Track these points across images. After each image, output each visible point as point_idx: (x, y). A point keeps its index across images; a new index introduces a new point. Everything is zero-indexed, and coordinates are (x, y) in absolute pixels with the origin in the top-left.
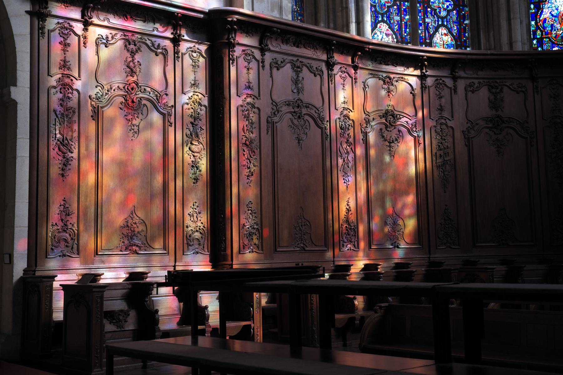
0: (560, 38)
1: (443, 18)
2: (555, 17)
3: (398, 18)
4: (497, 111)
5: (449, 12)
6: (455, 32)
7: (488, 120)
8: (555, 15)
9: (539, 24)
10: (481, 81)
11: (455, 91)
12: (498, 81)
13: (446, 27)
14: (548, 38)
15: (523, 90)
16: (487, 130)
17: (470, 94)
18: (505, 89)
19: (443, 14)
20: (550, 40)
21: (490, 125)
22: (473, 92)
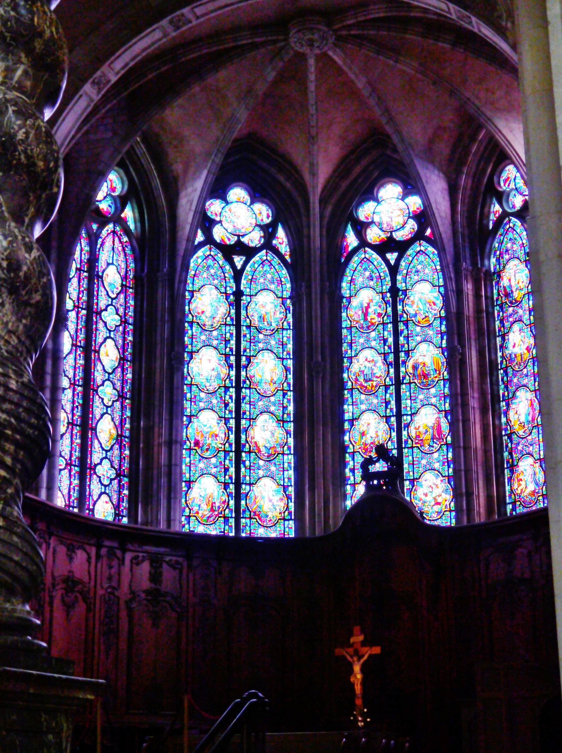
0: (205, 518)
1: (105, 486)
2: (204, 497)
3: (68, 482)
4: (156, 584)
5: (111, 480)
6: (115, 501)
7: (147, 592)
8: (203, 496)
9: (188, 502)
10: (143, 554)
11: (123, 563)
12: (159, 556)
13: (108, 494)
14: (195, 516)
15: (179, 566)
16: (145, 602)
17: (134, 566)
18: (165, 565)
19: (106, 482)
20: (197, 519)
21: (149, 598)
22: (138, 564)
